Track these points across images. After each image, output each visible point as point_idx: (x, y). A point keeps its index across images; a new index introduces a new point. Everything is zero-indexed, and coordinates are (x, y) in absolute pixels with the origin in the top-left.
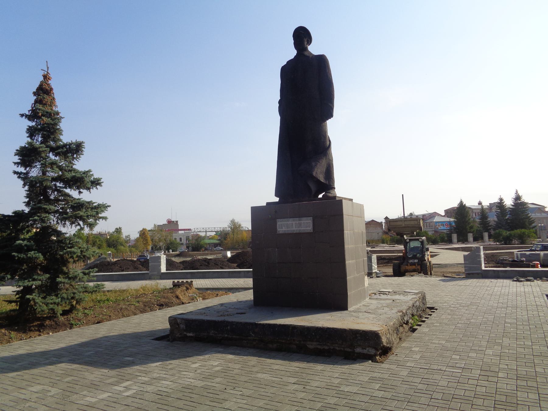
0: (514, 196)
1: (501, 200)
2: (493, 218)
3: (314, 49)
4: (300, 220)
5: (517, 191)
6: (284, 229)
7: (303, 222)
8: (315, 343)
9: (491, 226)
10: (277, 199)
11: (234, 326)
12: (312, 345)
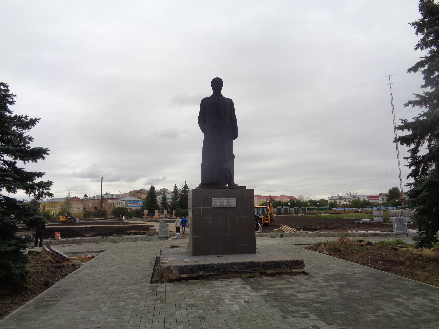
0: (183, 185)
1: (176, 187)
2: (170, 199)
4: (228, 200)
5: (186, 182)
6: (217, 205)
8: (270, 270)
9: (168, 205)
12: (269, 272)
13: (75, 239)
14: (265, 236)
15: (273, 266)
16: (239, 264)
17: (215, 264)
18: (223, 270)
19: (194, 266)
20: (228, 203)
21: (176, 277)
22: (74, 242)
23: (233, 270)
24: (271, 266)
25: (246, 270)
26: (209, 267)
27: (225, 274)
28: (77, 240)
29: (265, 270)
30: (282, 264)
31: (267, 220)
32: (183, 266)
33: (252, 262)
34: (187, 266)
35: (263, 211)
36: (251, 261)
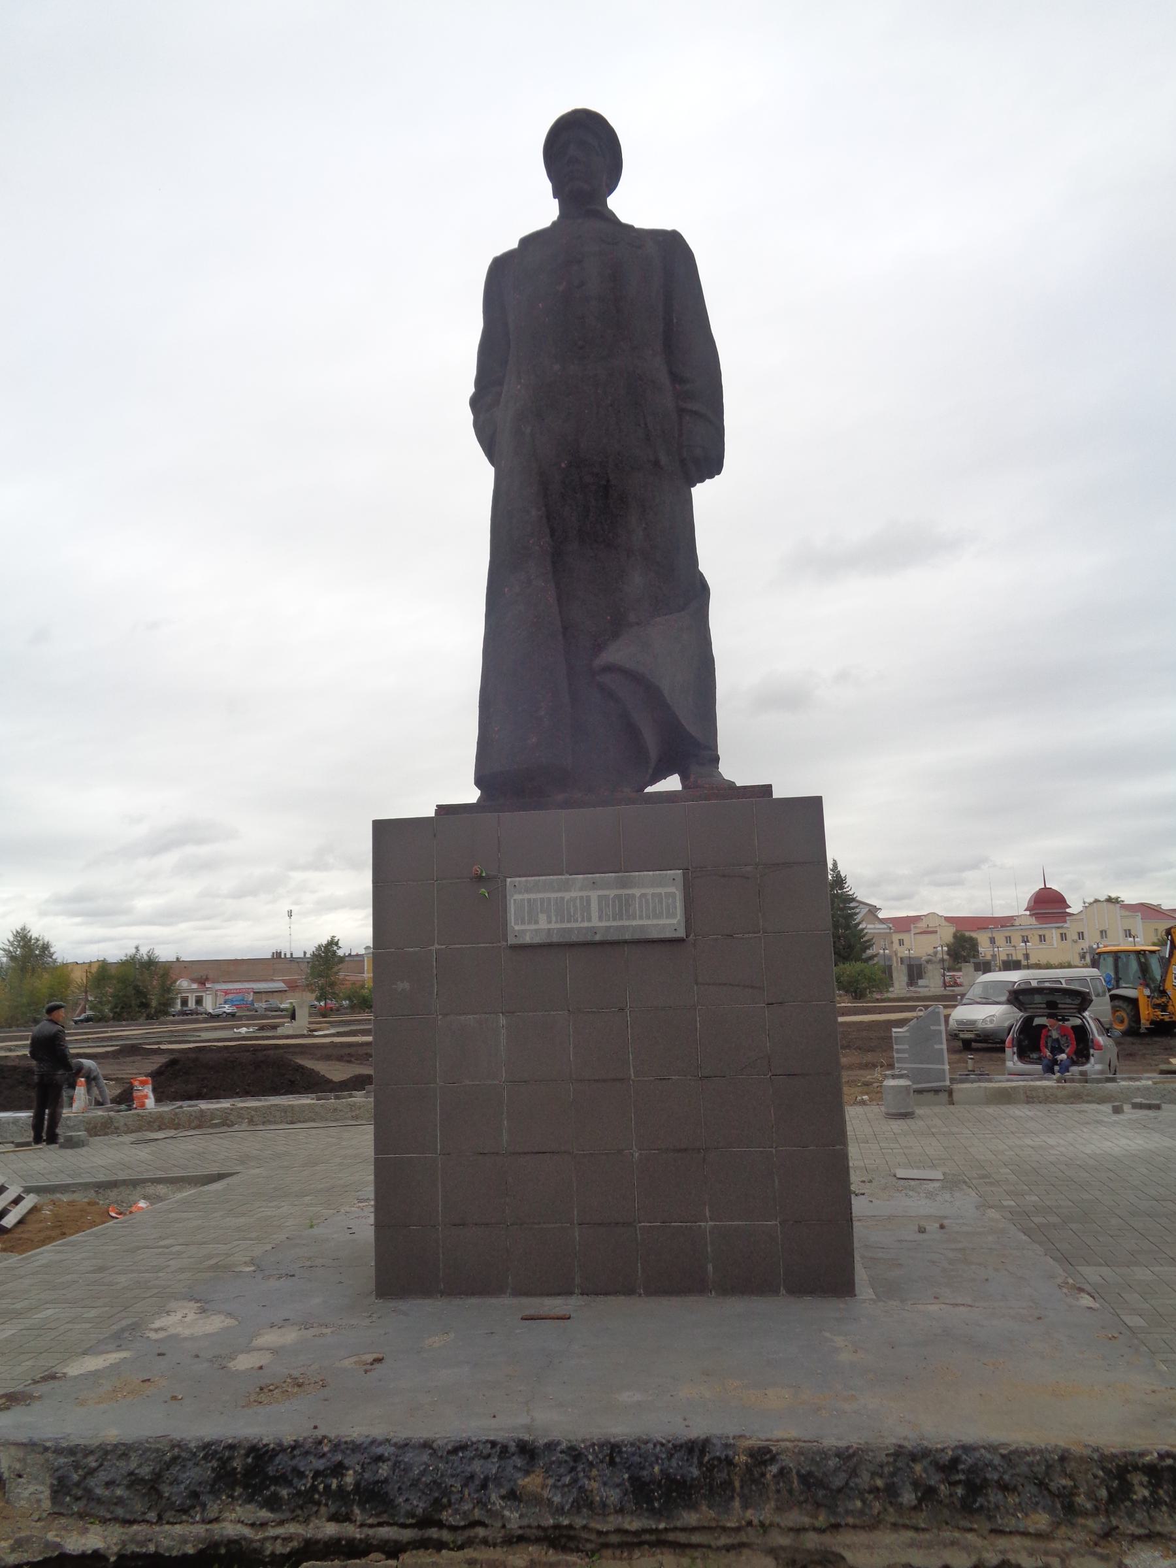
3: (634, 204)
4: (624, 885)
6: (543, 924)
7: (637, 892)
8: (887, 1537)
10: (471, 795)
11: (384, 1470)
13: (204, 1105)
14: (1101, 1101)
15: (908, 1497)
16: (575, 1454)
17: (356, 1447)
18: (420, 1505)
19: (174, 1456)
20: (623, 906)
21: (18, 1545)
22: (201, 1122)
23: (514, 1518)
24: (891, 1491)
25: (633, 1524)
26: (301, 1475)
27: (440, 1546)
28: (213, 1113)
29: (836, 1527)
30: (1005, 1488)
31: (1164, 1008)
32: (88, 1452)
33: (696, 1448)
34: (123, 1451)
35: (1144, 969)
36: (698, 1429)
